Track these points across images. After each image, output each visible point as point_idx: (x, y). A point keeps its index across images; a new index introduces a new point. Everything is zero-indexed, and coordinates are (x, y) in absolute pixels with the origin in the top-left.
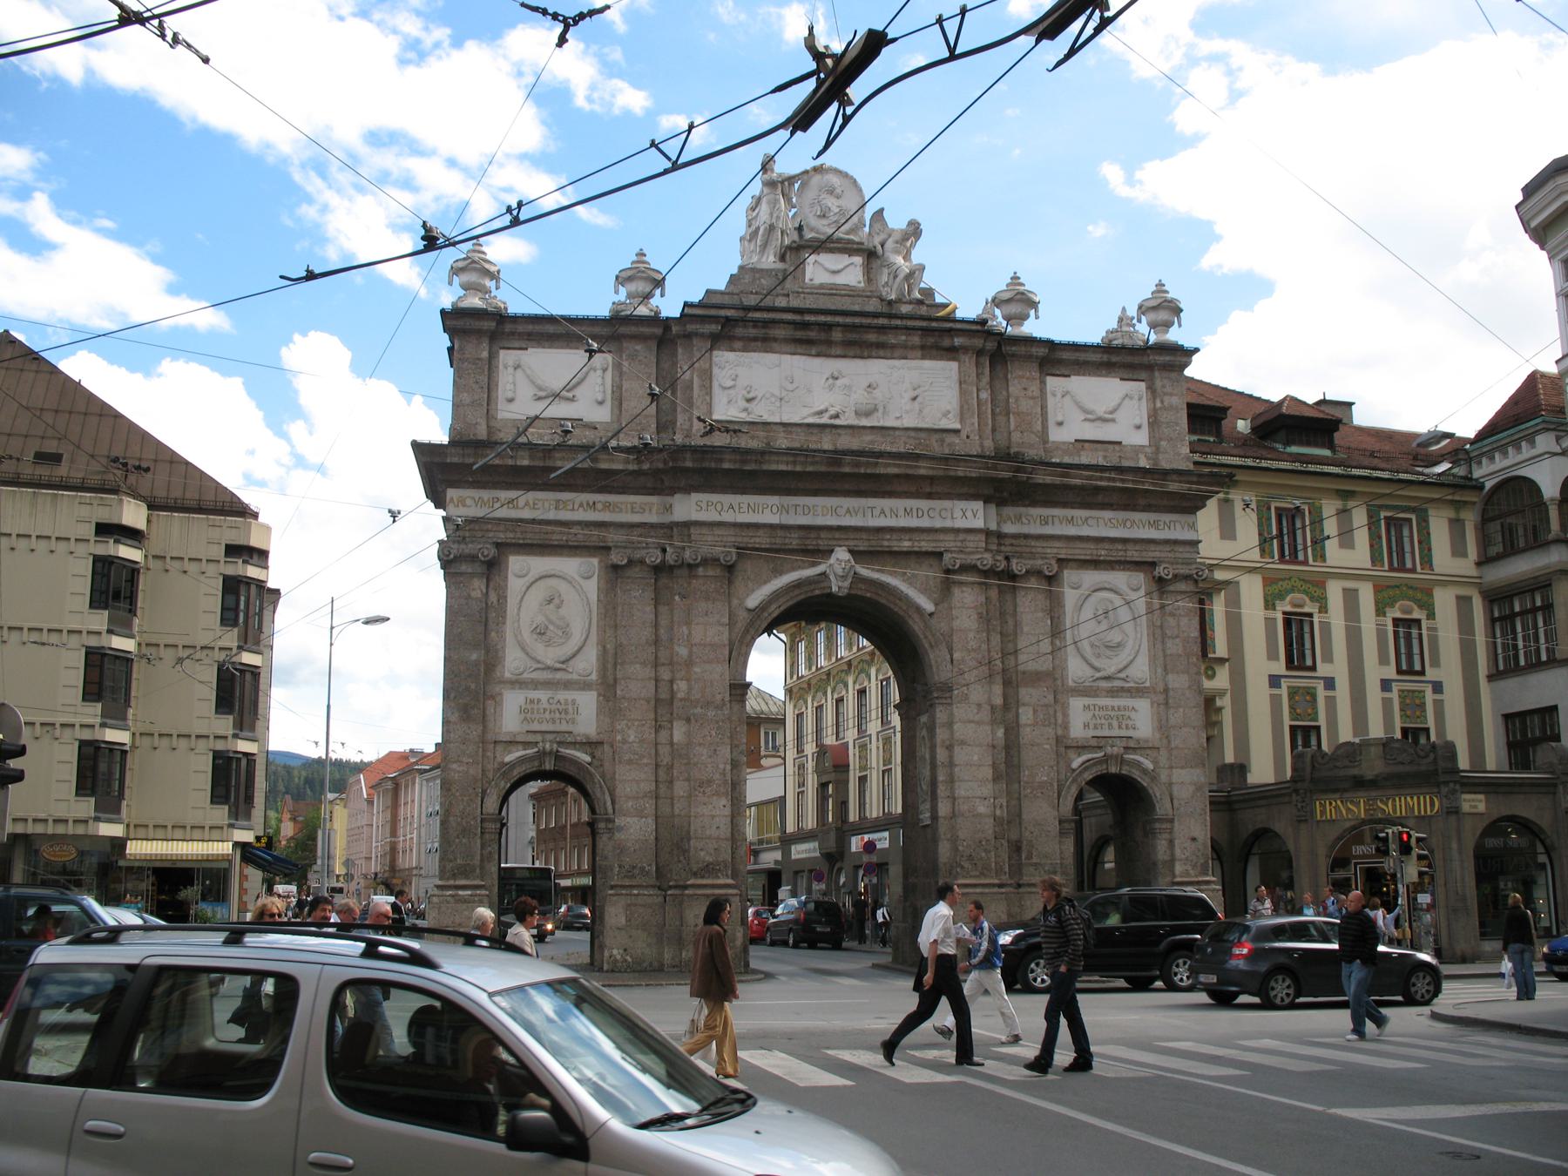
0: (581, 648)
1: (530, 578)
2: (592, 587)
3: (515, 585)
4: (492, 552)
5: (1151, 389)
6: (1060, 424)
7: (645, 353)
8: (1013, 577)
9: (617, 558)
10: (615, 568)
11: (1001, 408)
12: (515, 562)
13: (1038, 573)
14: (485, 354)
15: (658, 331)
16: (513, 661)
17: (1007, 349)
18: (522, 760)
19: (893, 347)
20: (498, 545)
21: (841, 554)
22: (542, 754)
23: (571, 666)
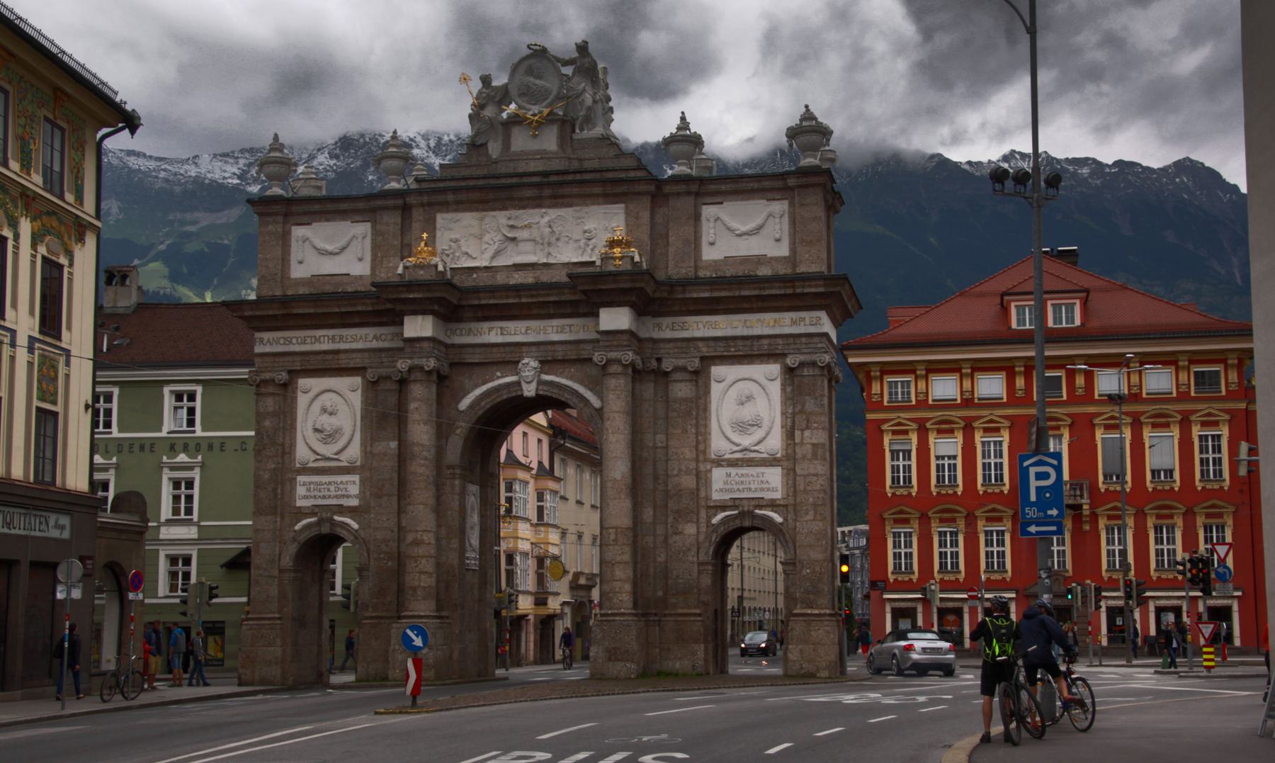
0: (349, 443)
1: (311, 395)
2: (356, 399)
3: (302, 400)
4: (284, 376)
5: (792, 205)
6: (712, 244)
7: (391, 221)
8: (666, 374)
9: (370, 375)
10: (374, 383)
11: (658, 238)
12: (303, 382)
13: (684, 369)
14: (280, 230)
15: (400, 202)
16: (302, 453)
17: (667, 189)
18: (308, 526)
19: (570, 196)
20: (290, 372)
21: (530, 364)
22: (319, 523)
23: (343, 457)
